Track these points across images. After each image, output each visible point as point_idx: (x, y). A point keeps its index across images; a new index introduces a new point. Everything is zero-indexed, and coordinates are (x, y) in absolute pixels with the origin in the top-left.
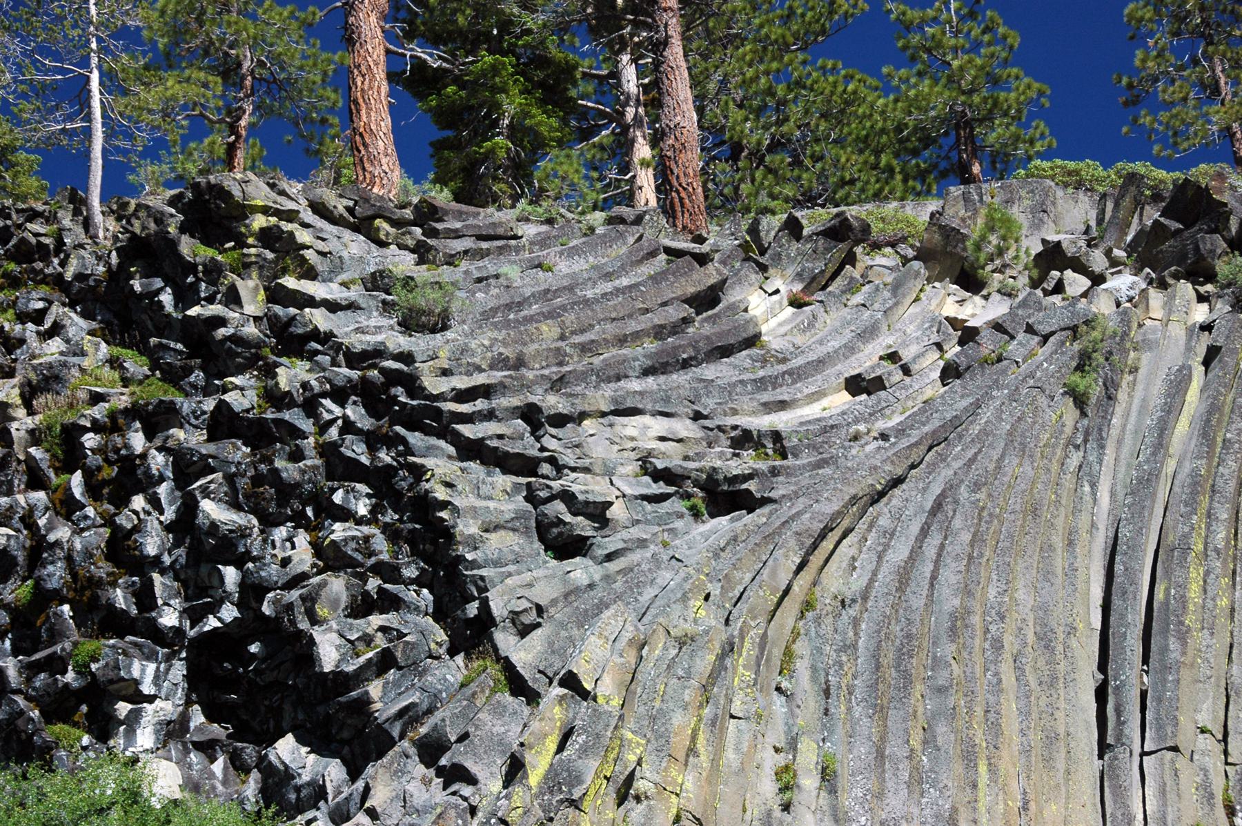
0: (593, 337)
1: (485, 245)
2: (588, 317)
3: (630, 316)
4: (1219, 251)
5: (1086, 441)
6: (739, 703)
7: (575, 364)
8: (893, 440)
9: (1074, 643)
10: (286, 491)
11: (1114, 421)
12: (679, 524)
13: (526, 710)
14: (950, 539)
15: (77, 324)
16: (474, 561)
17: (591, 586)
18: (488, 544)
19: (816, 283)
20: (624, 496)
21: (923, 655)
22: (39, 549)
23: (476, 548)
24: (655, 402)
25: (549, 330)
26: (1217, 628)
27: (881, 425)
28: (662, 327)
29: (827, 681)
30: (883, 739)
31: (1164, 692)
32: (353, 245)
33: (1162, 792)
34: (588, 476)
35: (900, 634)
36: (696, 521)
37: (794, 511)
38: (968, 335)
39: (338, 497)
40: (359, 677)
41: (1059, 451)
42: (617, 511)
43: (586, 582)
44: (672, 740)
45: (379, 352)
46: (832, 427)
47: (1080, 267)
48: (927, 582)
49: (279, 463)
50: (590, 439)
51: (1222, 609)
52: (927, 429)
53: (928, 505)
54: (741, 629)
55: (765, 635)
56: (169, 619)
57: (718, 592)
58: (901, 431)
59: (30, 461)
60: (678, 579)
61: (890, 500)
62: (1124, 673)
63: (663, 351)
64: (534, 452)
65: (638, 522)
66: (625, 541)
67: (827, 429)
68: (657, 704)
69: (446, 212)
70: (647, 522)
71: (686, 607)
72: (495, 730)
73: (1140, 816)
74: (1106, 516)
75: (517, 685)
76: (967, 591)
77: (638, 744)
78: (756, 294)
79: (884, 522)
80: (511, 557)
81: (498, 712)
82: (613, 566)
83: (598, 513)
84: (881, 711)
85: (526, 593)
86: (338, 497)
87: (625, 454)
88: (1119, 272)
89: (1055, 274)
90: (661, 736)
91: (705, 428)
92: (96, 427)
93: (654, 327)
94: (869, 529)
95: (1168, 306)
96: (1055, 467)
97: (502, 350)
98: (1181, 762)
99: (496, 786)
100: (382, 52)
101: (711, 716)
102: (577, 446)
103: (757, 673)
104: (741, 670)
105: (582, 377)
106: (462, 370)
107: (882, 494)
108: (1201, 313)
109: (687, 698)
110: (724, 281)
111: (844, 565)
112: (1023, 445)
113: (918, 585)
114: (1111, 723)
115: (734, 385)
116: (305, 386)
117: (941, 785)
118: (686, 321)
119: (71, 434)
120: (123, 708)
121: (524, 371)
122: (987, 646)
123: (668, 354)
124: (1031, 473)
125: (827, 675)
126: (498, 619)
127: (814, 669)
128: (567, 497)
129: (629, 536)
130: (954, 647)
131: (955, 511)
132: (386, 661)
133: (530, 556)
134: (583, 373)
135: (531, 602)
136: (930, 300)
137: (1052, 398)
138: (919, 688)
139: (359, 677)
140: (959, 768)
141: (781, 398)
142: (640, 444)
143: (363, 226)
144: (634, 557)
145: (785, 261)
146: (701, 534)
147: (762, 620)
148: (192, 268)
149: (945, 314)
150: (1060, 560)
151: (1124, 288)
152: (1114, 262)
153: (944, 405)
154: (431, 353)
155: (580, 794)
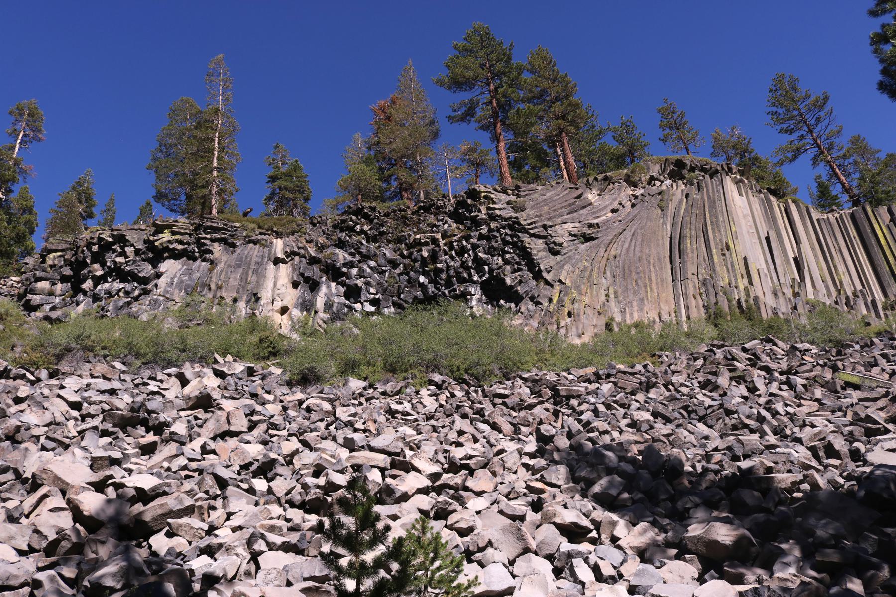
10: (495, 249)
15: (450, 221)
19: (602, 190)
22: (448, 267)
25: (546, 208)
27: (620, 219)
32: (503, 196)
33: (686, 287)
38: (636, 197)
39: (506, 249)
40: (515, 285)
42: (565, 244)
45: (511, 218)
47: (658, 180)
49: (493, 243)
56: (476, 278)
58: (624, 219)
59: (444, 250)
75: (547, 282)
76: (641, 251)
79: (623, 239)
81: (545, 289)
82: (565, 256)
83: (561, 245)
86: (506, 249)
92: (456, 241)
95: (677, 186)
98: (689, 281)
99: (546, 305)
104: (595, 274)
105: (554, 217)
108: (683, 187)
116: (497, 227)
118: (576, 202)
119: (451, 243)
120: (469, 297)
128: (554, 243)
132: (520, 282)
138: (634, 273)
139: (515, 285)
140: (643, 289)
143: (505, 191)
144: (570, 254)
148: (470, 206)
152: (665, 178)
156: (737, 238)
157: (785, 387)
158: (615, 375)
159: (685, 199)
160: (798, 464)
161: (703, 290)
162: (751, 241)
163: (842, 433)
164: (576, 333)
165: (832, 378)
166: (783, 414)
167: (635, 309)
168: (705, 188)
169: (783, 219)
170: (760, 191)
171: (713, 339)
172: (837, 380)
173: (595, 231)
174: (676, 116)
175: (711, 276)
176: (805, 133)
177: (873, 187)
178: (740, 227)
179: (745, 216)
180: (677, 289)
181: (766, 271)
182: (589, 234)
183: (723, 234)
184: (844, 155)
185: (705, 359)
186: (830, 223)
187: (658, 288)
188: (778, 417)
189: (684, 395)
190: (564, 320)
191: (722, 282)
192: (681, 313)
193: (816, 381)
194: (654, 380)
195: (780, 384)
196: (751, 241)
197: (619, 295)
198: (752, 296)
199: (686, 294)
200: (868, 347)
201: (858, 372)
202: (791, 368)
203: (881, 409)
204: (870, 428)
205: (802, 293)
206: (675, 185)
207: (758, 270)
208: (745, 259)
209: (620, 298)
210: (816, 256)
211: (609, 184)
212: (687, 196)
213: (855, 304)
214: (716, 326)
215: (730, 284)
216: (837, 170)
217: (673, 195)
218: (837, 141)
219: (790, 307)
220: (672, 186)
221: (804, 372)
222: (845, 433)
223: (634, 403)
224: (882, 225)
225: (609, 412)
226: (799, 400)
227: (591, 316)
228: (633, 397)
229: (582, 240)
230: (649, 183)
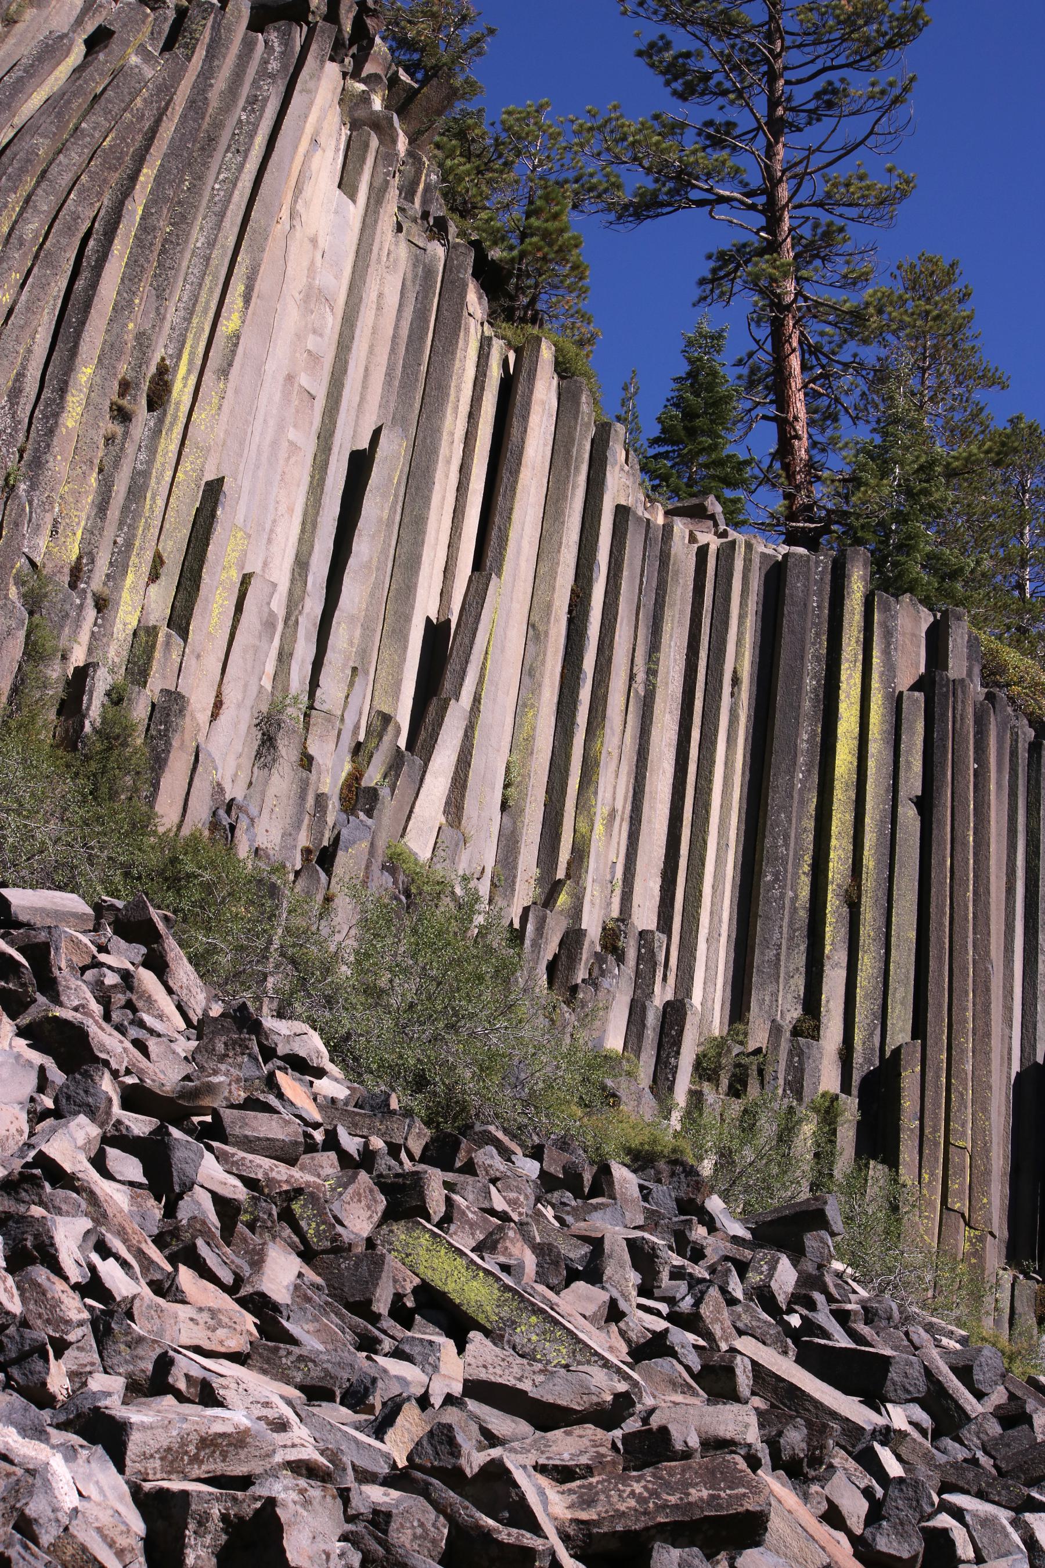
156: (224, 372)
157: (130, 1167)
159: (79, 50)
160: (53, 1549)
162: (281, 428)
163: (344, 1495)
165: (370, 1243)
166: (75, 1275)
168: (200, 53)
169: (473, 417)
170: (438, 229)
172: (392, 1261)
176: (745, 122)
177: (900, 517)
178: (268, 335)
179: (313, 296)
181: (278, 605)
183: (172, 315)
184: (857, 317)
186: (664, 558)
188: (41, 1274)
191: (43, 542)
193: (287, 1216)
195: (106, 1140)
196: (281, 428)
198: (156, 683)
200: (578, 1194)
201: (506, 1268)
202: (195, 1094)
203: (562, 1474)
204: (487, 1535)
205: (389, 805)
207: (246, 580)
208: (213, 491)
210: (529, 672)
212: (99, 40)
213: (592, 982)
215: (76, 573)
216: (795, 362)
218: (857, 235)
219: (303, 840)
221: (250, 1145)
222: (358, 1505)
224: (875, 684)
226: (173, 1260)
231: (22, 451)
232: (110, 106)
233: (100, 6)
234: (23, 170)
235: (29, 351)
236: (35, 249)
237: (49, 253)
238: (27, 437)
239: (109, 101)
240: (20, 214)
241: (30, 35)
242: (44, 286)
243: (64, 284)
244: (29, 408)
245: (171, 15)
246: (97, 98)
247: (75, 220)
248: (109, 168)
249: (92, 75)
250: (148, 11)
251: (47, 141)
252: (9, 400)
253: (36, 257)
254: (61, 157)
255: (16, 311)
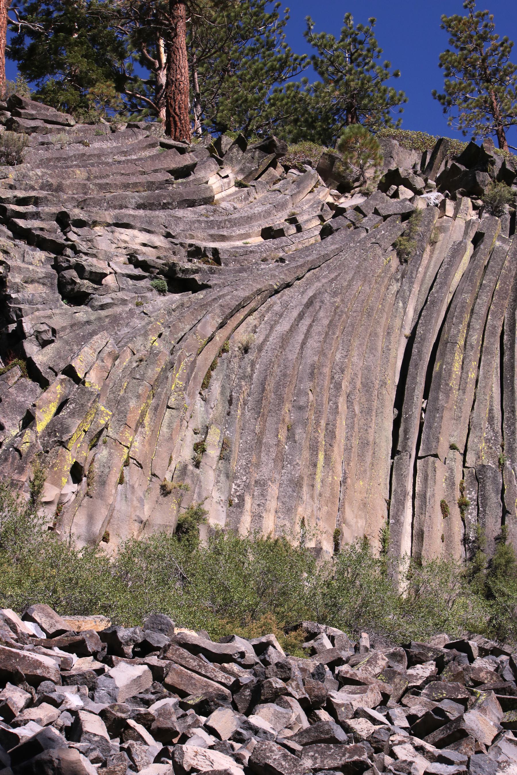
0: (108, 182)
1: (49, 126)
2: (106, 170)
3: (133, 174)
4: (487, 182)
5: (403, 277)
6: (173, 400)
7: (94, 194)
8: (287, 262)
9: (384, 392)
11: (420, 269)
12: (149, 295)
13: (39, 390)
14: (316, 322)
16: (16, 299)
17: (88, 322)
18: (26, 290)
20: (116, 273)
21: (292, 387)
23: (18, 292)
24: (142, 223)
25: (80, 174)
26: (468, 389)
27: (281, 254)
28: (153, 183)
29: (231, 396)
30: (262, 433)
31: (434, 423)
33: (426, 479)
34: (95, 259)
35: (279, 374)
36: (160, 294)
37: (221, 294)
38: (340, 212)
41: (386, 280)
42: (109, 280)
43: (85, 320)
44: (128, 415)
46: (251, 252)
47: (409, 185)
48: (298, 346)
50: (98, 238)
51: (471, 380)
52: (309, 258)
53: (305, 300)
54: (180, 357)
55: (194, 362)
57: (167, 334)
58: (292, 258)
60: (143, 323)
61: (282, 296)
62: (412, 411)
63: (152, 196)
64: (61, 240)
65: (123, 289)
66: (113, 299)
67: (248, 252)
68: (122, 393)
69: (27, 105)
70: (129, 290)
71: (146, 340)
72: (18, 399)
73: (411, 494)
74: (410, 322)
76: (322, 353)
77: (108, 414)
78: (214, 176)
79: (277, 308)
80: (40, 300)
81: (22, 388)
82: (103, 313)
84: (263, 416)
85: (47, 321)
87: (120, 250)
88: (431, 191)
89: (394, 187)
90: (122, 412)
91: (172, 242)
93: (148, 182)
94: (269, 309)
96: (383, 289)
97: (49, 179)
98: (438, 463)
99: (15, 431)
100: (5, 22)
101: (154, 405)
102: (89, 241)
103: (187, 383)
105: (98, 203)
106: (23, 187)
107: (277, 292)
108: (473, 215)
109: (140, 392)
110: (195, 165)
111: (249, 329)
112: (365, 276)
113: (293, 347)
114: (401, 439)
115: (194, 222)
117: (295, 463)
121: (61, 194)
122: (332, 386)
123: (154, 199)
124: (368, 290)
125: (232, 392)
126: (27, 334)
127: (223, 387)
128: (80, 268)
129: (116, 296)
130: (311, 384)
131: (320, 307)
133: (52, 301)
134: (99, 200)
135: (49, 327)
136: (319, 192)
137: (385, 251)
138: (287, 406)
140: (306, 454)
141: (222, 233)
142: (130, 246)
144: (118, 310)
145: (235, 162)
146: (161, 301)
147: (194, 353)
149: (327, 201)
150: (381, 343)
151: (433, 198)
153: (320, 247)
154: (3, 174)
155: (67, 438)
158: (166, 649)
159: (470, 247)
161: (471, 495)
164: (83, 531)
167: (273, 504)
171: (473, 631)
173: (205, 267)
174: (487, 49)
175: (501, 465)
180: (401, 478)
182: (185, 271)
185: (441, 664)
187: (347, 461)
189: (358, 739)
190: (57, 483)
192: (398, 545)
194: (279, 684)
197: (235, 455)
199: (424, 496)
206: (450, 206)
209: (235, 466)
211: (273, 164)
212: (478, 240)
214: (489, 595)
217: (441, 229)
220: (442, 206)
223: (200, 732)
225: (116, 743)
227: (140, 493)
228: (203, 719)
229: (163, 282)
230: (383, 187)
231: (502, 446)
232: (494, 269)
233: (474, 223)
234: (462, 312)
235: (491, 397)
236: (479, 348)
237: (487, 348)
238: (503, 439)
239: (492, 267)
240: (467, 333)
241: (445, 247)
242: (489, 364)
243: (498, 360)
244: (500, 424)
245: (508, 217)
246: (486, 267)
247: (494, 328)
248: (503, 299)
249: (480, 257)
250: (497, 218)
251: (469, 295)
252: (489, 423)
253: (481, 351)
254: (478, 300)
255: (479, 380)
